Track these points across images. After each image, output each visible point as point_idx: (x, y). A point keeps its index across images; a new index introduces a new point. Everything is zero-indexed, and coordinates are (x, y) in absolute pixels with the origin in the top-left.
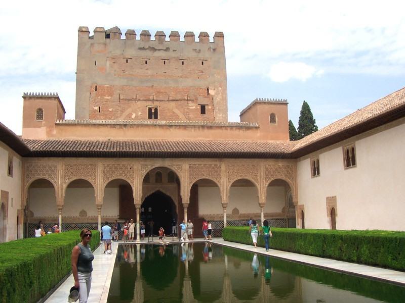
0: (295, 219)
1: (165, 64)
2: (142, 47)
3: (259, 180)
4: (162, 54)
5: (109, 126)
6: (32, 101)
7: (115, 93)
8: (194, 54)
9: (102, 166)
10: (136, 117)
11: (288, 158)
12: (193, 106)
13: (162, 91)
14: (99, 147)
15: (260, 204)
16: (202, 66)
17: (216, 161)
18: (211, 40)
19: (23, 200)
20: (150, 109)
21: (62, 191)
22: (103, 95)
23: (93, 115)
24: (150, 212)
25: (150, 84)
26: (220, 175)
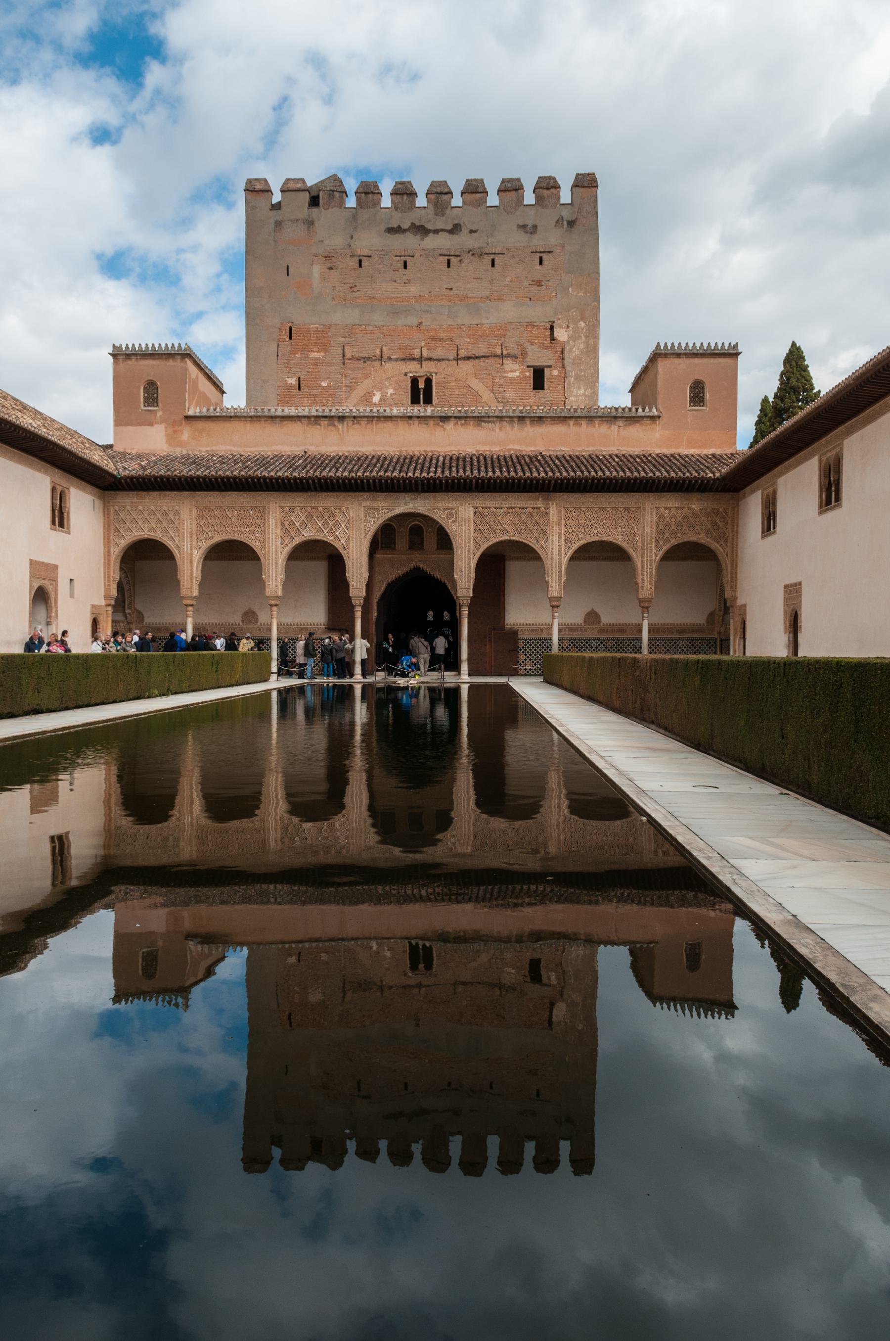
0: (728, 640)
1: (449, 266)
2: (395, 226)
4: (442, 242)
5: (305, 421)
6: (132, 362)
9: (279, 510)
11: (717, 491)
14: (272, 467)
15: (641, 601)
16: (539, 267)
18: (565, 196)
19: (109, 585)
20: (414, 381)
21: (192, 566)
22: (306, 349)
24: (447, 621)
25: (413, 320)
26: (545, 533)
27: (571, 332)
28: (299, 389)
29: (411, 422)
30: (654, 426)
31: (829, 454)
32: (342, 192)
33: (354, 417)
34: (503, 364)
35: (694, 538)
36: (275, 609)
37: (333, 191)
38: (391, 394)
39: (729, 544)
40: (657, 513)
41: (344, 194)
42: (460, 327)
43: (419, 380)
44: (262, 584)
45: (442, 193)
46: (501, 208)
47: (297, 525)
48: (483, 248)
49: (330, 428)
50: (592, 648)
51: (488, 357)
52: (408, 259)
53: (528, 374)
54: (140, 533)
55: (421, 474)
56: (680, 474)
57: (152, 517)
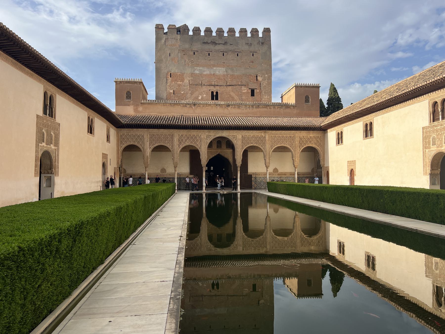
0: (322, 177)
1: (223, 55)
8: (246, 48)
12: (245, 90)
16: (252, 57)
18: (260, 35)
20: (212, 93)
22: (176, 80)
24: (212, 170)
27: (263, 78)
28: (174, 94)
30: (294, 109)
33: (198, 104)
35: (311, 145)
40: (300, 137)
46: (240, 37)
47: (184, 141)
49: (190, 108)
52: (210, 53)
53: (249, 91)
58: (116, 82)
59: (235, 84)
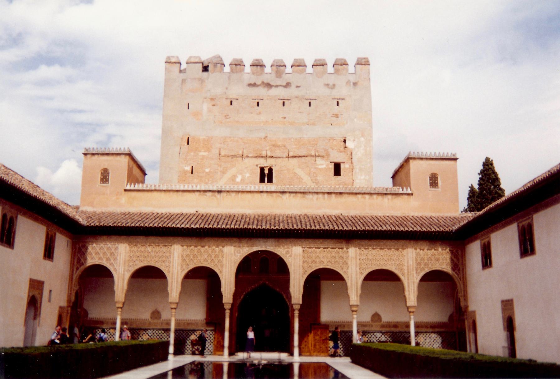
1: (284, 105)
2: (253, 83)
3: (406, 271)
5: (197, 194)
7: (213, 147)
10: (242, 180)
12: (323, 165)
13: (280, 143)
14: (177, 222)
15: (408, 308)
17: (341, 243)
19: (71, 294)
20: (262, 169)
21: (123, 282)
23: (182, 178)
25: (263, 135)
26: (347, 263)
28: (192, 173)
29: (262, 194)
31: (524, 223)
32: (222, 64)
33: (228, 191)
34: (316, 161)
36: (174, 310)
37: (217, 63)
38: (248, 177)
39: (461, 273)
41: (223, 65)
42: (290, 139)
43: (265, 168)
44: (168, 294)
45: (280, 66)
48: (304, 96)
50: (377, 337)
51: (307, 156)
54: (93, 261)
55: (270, 227)
56: (429, 229)
57: (102, 251)
58: (85, 154)
59: (304, 155)
